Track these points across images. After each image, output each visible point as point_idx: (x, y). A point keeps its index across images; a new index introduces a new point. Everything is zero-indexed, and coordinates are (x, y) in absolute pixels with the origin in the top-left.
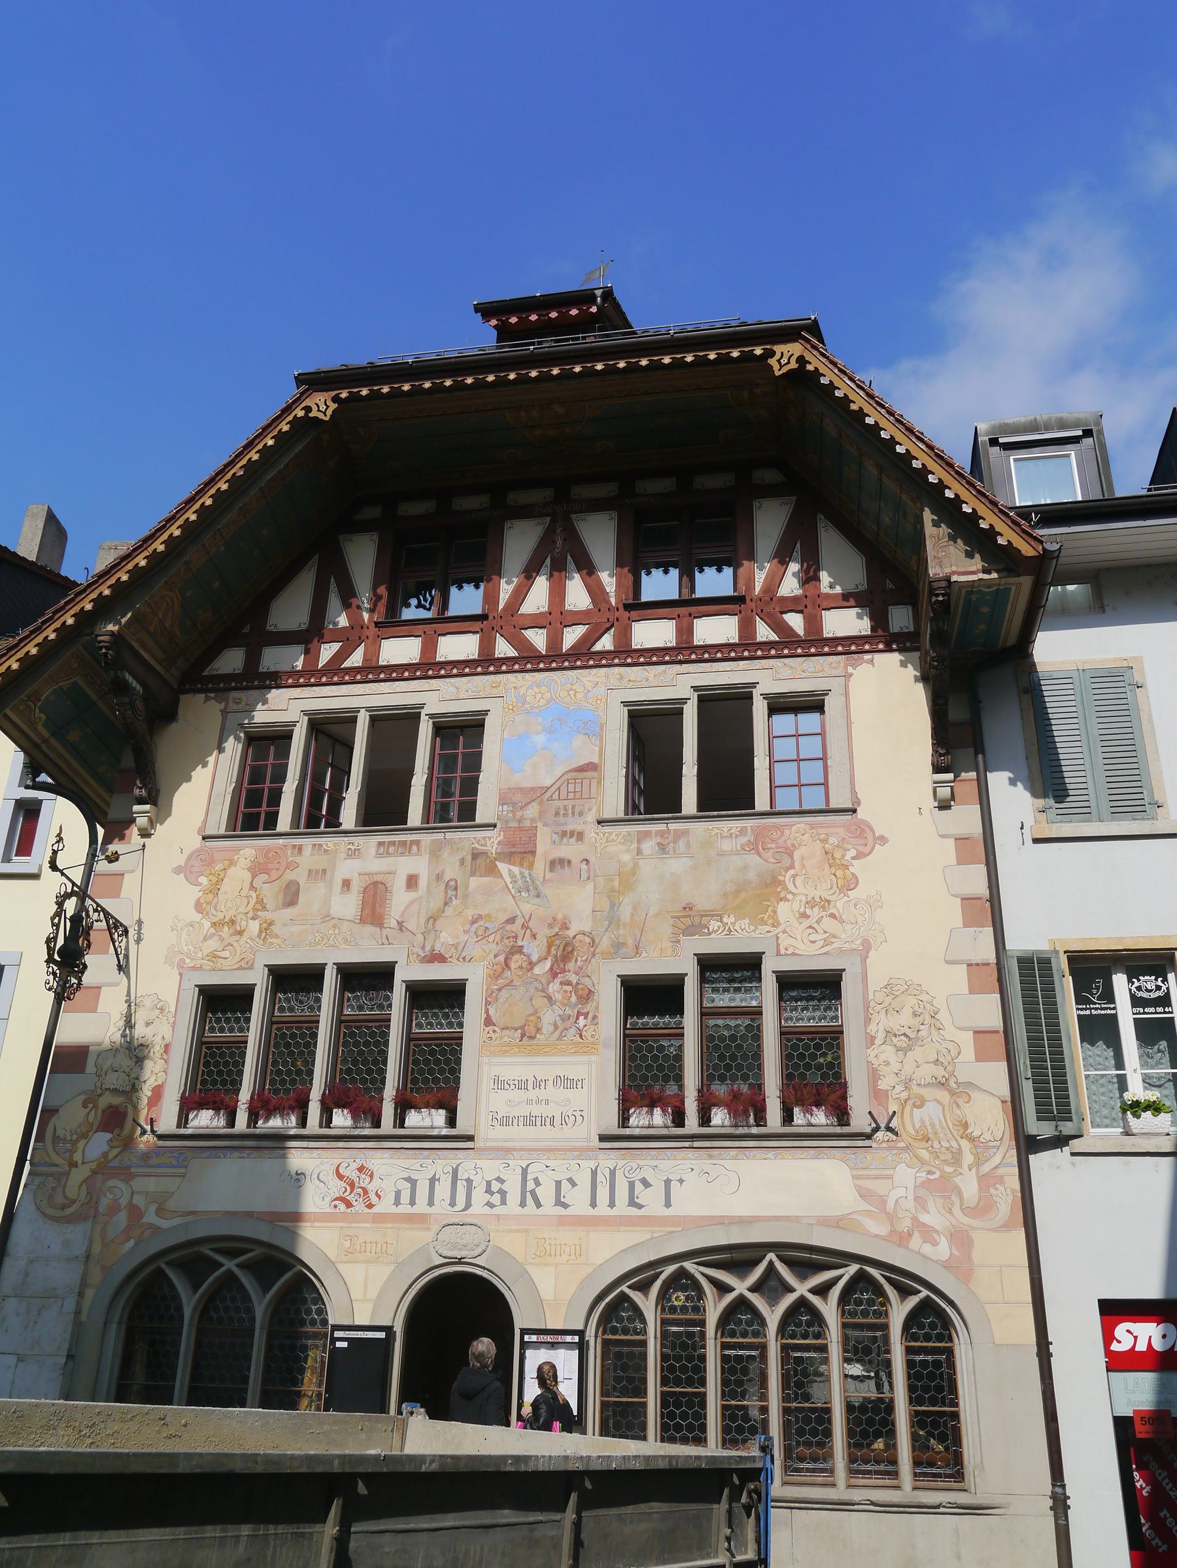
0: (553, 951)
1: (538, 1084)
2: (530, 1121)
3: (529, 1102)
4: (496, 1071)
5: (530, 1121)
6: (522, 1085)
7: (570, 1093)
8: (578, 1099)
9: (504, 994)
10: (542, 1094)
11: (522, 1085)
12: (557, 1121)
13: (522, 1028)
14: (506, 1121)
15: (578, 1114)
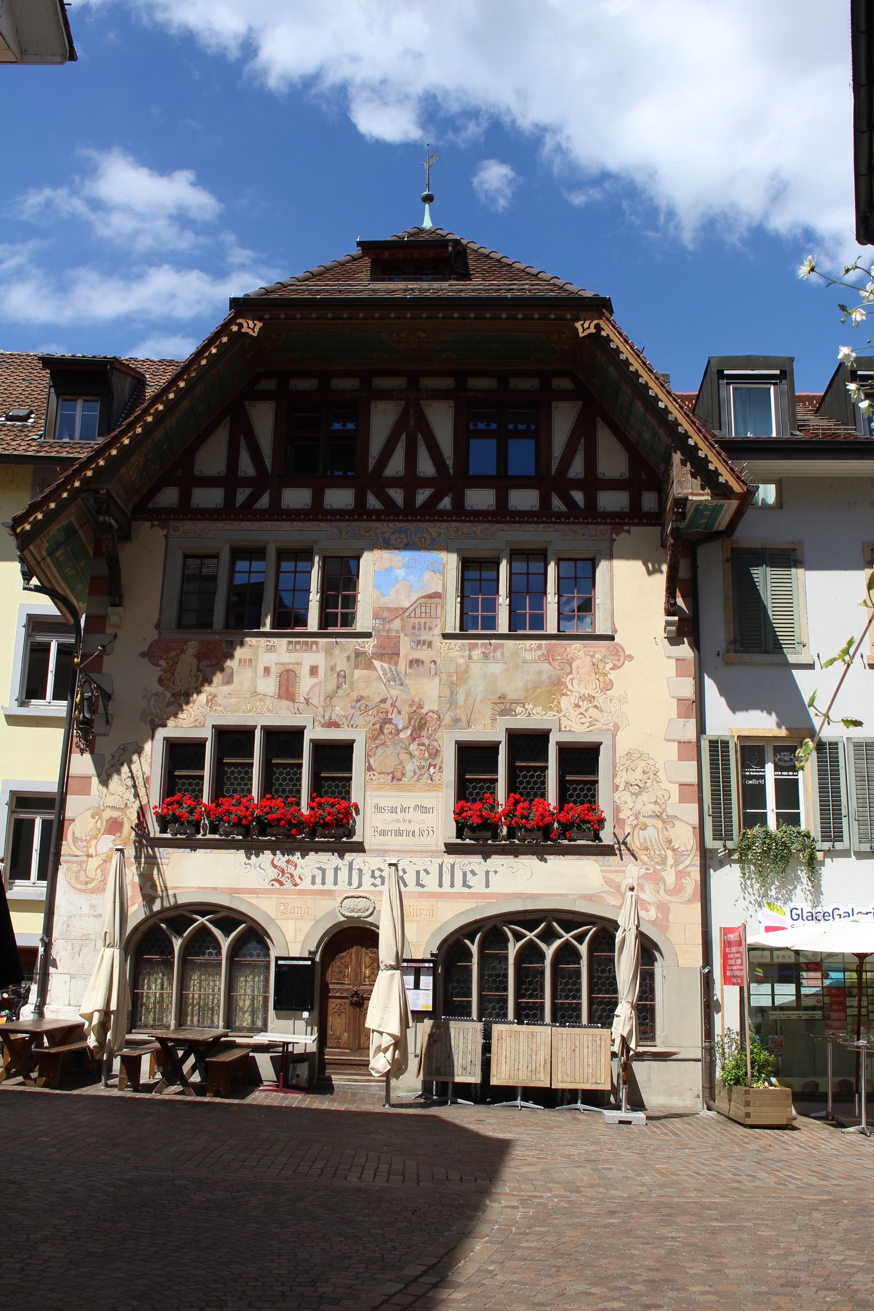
0: (412, 723)
1: (403, 810)
2: (399, 833)
3: (398, 821)
4: (375, 801)
5: (399, 833)
6: (393, 810)
7: (424, 816)
8: (430, 820)
9: (380, 751)
10: (407, 816)
11: (393, 810)
12: (417, 834)
13: (393, 773)
14: (383, 833)
15: (430, 829)
